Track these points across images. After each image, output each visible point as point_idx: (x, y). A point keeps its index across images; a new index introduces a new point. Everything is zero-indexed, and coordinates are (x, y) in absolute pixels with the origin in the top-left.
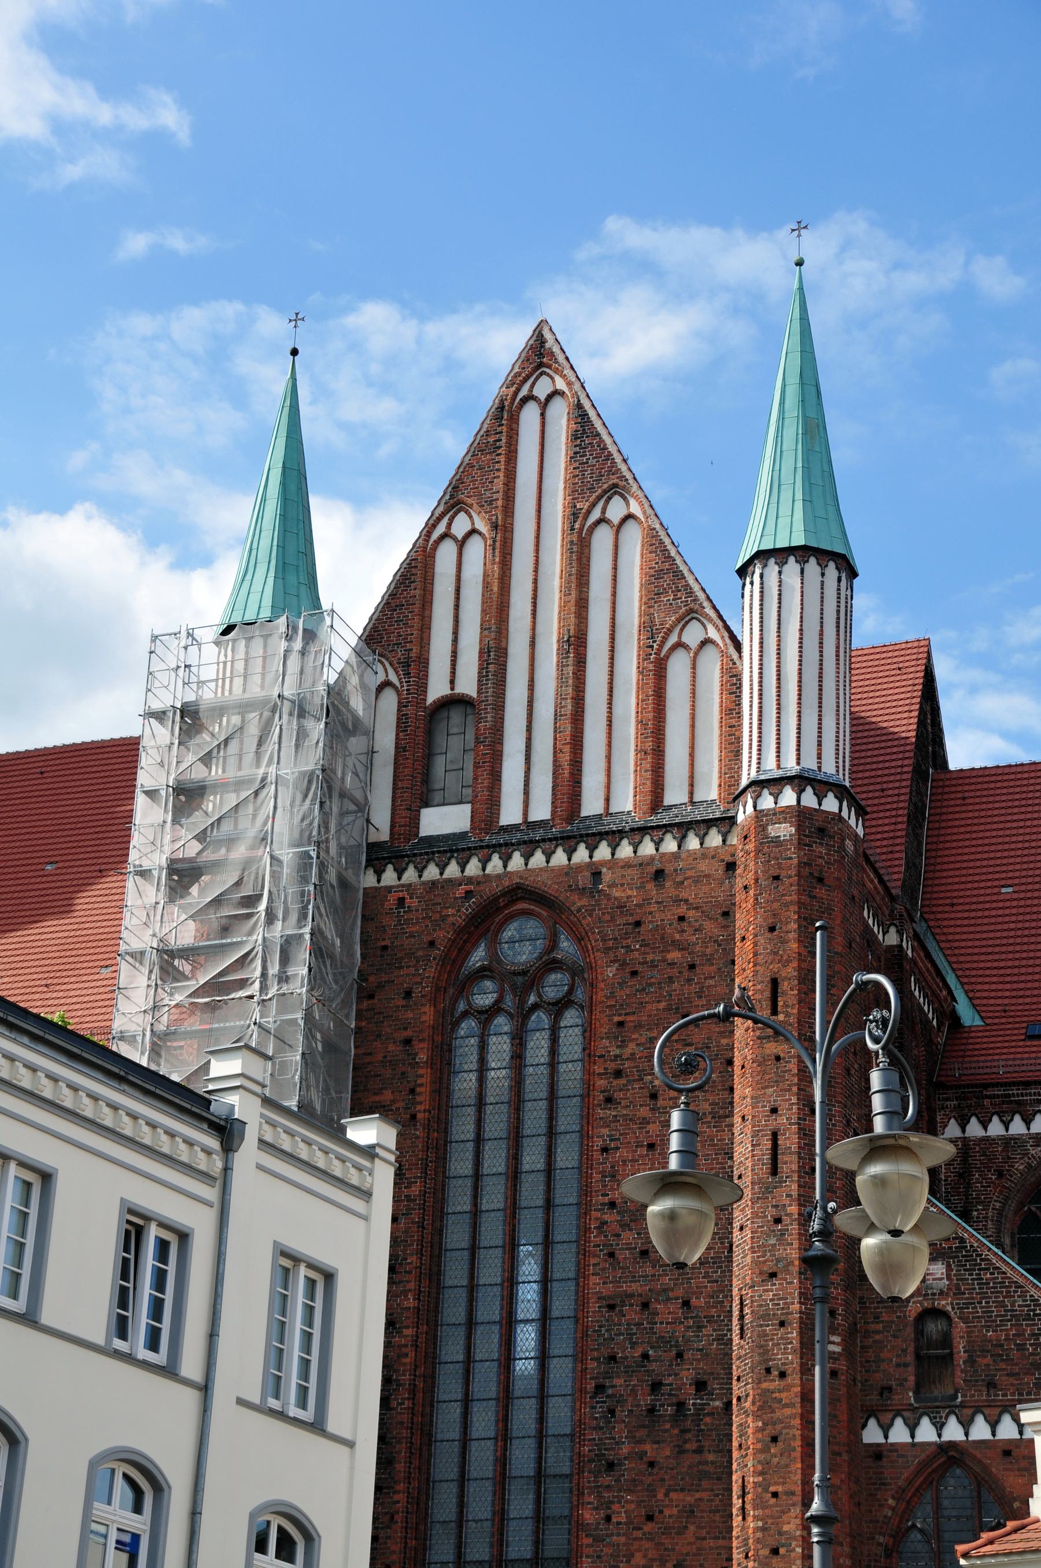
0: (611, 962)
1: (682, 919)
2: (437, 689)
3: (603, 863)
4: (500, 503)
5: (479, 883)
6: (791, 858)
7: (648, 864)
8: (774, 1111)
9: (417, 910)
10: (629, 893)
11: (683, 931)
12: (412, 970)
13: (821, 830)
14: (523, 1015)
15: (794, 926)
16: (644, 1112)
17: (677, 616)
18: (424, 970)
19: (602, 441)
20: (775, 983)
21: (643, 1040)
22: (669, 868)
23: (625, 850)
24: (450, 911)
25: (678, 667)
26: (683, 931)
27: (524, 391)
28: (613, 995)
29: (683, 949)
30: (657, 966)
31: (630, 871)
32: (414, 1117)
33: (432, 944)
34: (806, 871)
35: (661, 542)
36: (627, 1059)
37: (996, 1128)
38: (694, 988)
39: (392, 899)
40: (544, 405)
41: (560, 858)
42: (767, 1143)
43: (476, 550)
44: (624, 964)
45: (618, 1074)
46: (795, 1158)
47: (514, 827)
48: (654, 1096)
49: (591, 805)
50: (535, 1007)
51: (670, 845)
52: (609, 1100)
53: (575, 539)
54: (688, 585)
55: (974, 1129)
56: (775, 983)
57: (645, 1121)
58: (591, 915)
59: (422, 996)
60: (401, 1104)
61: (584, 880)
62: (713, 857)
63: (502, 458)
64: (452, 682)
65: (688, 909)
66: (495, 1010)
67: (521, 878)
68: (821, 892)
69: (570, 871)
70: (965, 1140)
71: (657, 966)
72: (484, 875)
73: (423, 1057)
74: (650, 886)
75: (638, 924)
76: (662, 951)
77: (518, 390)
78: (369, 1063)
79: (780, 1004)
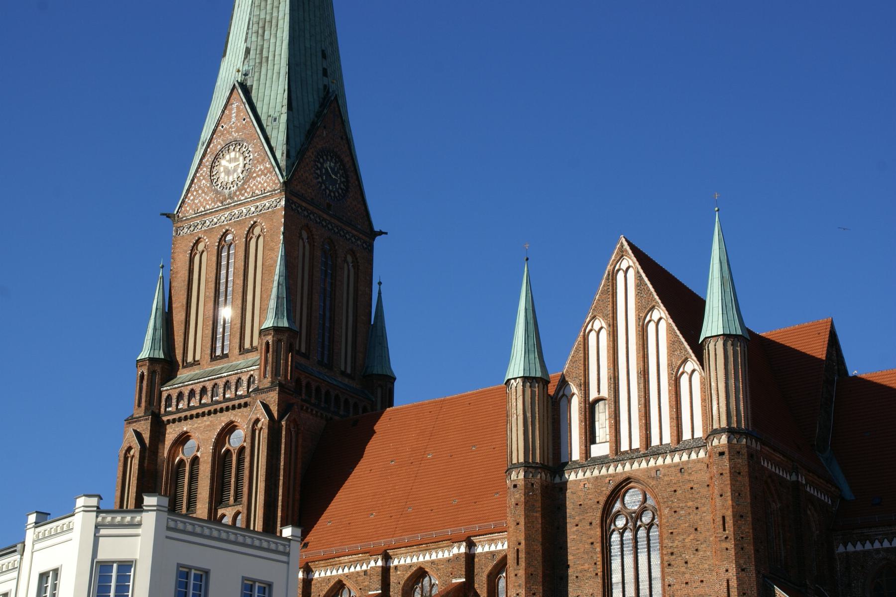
0: (666, 507)
1: (692, 488)
2: (593, 395)
3: (660, 466)
4: (611, 315)
5: (614, 476)
6: (726, 466)
7: (677, 466)
8: (727, 571)
9: (591, 489)
10: (671, 478)
11: (693, 493)
12: (591, 514)
13: (739, 452)
14: (636, 530)
15: (729, 494)
16: (683, 569)
17: (682, 360)
19: (648, 287)
20: (724, 518)
21: (681, 540)
22: (685, 467)
23: (668, 460)
24: (604, 489)
25: (684, 380)
26: (693, 493)
27: (617, 267)
28: (668, 522)
29: (693, 501)
30: (683, 508)
31: (670, 469)
32: (597, 574)
33: (598, 502)
34: (732, 471)
35: (674, 329)
36: (675, 548)
37: (859, 547)
38: (698, 517)
39: (582, 484)
40: (626, 272)
41: (644, 464)
42: (725, 584)
43: (604, 335)
44: (671, 508)
45: (672, 554)
46: (736, 590)
47: (626, 452)
48: (686, 563)
49: (655, 442)
50: (640, 526)
51: (685, 457)
52: (669, 565)
53: (640, 329)
54: (685, 347)
55: (850, 548)
56: (724, 518)
57: (684, 573)
58: (657, 488)
60: (591, 569)
61: (653, 474)
62: (702, 462)
63: (610, 296)
64: (599, 391)
65: (694, 484)
66: (625, 529)
67: (630, 473)
68: (739, 478)
69: (648, 470)
70: (847, 553)
71: (683, 508)
73: (599, 549)
74: (679, 474)
75: (675, 491)
76: (685, 502)
77: (615, 267)
78: (579, 553)
79: (726, 526)
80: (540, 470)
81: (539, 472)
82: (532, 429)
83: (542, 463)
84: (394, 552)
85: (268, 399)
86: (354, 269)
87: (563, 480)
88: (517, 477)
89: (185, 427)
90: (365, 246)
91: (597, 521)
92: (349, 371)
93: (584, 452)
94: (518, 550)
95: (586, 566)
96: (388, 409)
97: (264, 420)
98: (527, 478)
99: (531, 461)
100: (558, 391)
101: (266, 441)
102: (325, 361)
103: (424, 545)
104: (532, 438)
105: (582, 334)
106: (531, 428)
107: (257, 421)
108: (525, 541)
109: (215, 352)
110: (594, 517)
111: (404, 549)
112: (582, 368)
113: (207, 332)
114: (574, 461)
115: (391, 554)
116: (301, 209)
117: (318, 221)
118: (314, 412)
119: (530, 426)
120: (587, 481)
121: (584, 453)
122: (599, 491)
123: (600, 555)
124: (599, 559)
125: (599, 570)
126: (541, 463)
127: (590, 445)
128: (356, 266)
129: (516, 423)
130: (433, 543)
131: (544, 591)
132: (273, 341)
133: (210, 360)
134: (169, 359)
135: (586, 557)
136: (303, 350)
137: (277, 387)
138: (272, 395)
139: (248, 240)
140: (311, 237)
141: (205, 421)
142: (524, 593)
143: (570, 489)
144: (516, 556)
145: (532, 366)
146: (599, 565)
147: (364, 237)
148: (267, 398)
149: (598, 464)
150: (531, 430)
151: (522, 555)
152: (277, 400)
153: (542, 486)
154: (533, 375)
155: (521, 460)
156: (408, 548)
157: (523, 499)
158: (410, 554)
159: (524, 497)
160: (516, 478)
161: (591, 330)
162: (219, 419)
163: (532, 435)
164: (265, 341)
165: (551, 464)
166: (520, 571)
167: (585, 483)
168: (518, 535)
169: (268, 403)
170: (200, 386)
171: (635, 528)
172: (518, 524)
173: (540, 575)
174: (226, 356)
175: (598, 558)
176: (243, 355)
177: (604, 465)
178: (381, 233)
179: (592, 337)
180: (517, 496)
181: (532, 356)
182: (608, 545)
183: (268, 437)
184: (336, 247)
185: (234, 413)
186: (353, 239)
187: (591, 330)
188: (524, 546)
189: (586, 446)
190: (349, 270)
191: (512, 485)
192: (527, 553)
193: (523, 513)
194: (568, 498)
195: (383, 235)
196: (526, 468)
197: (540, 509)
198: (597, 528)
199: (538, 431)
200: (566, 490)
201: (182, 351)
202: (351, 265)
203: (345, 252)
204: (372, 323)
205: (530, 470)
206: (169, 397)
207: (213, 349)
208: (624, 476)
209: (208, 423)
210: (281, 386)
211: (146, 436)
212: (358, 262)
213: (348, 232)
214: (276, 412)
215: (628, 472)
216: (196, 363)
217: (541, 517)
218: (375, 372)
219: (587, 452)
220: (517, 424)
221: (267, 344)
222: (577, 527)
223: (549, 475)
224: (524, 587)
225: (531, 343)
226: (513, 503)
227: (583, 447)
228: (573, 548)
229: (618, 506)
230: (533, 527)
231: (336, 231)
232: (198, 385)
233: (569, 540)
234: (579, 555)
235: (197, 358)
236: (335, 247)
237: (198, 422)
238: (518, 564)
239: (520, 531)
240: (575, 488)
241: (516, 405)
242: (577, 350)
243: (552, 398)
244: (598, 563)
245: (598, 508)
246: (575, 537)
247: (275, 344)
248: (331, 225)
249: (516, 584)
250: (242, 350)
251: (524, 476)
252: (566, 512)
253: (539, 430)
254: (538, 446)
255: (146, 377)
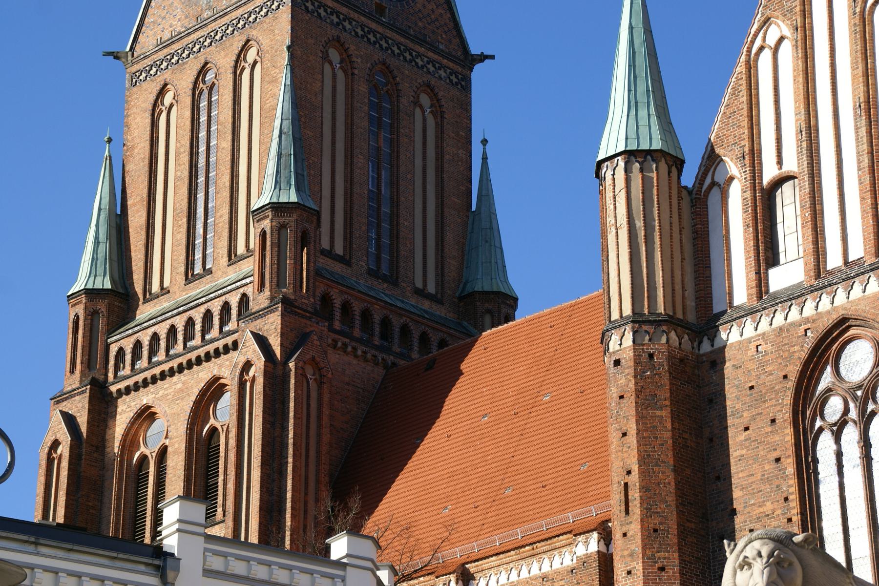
2: (770, 172)
4: (798, 9)
5: (814, 321)
9: (772, 353)
12: (774, 402)
18: (783, 399)
24: (796, 348)
32: (790, 520)
39: (753, 346)
43: (787, 52)
53: (857, 22)
59: (784, 421)
64: (780, 162)
67: (845, 309)
72: (817, 314)
78: (752, 483)
80: (665, 328)
81: (663, 331)
82: (646, 251)
83: (671, 314)
84: (477, 566)
85: (267, 327)
86: (435, 117)
87: (717, 345)
88: (621, 345)
89: (145, 397)
90: (455, 80)
91: (785, 415)
92: (431, 288)
93: (754, 284)
94: (626, 484)
95: (769, 507)
96: (484, 333)
97: (259, 362)
98: (640, 345)
99: (646, 312)
100: (701, 178)
101: (262, 398)
102: (385, 270)
103: (527, 548)
104: (647, 267)
105: (743, 58)
106: (644, 248)
107: (248, 365)
108: (640, 466)
109: (193, 269)
110: (779, 408)
111: (494, 558)
112: (745, 123)
113: (179, 236)
114: (738, 307)
115: (472, 570)
116: (325, 11)
117: (360, 33)
118: (359, 352)
119: (644, 244)
120: (763, 338)
121: (754, 285)
122: (786, 354)
123: (793, 482)
124: (792, 490)
125: (795, 511)
126: (666, 314)
127: (767, 270)
128: (438, 112)
129: (615, 244)
130: (542, 541)
131: (682, 562)
132: (272, 227)
133: (184, 282)
134: (121, 291)
135: (767, 488)
136: (339, 249)
137: (280, 305)
138: (271, 320)
139: (238, 72)
140: (347, 62)
141: (175, 383)
142: (641, 568)
143: (730, 360)
144: (623, 498)
145: (644, 131)
146: (793, 500)
147: (451, 65)
148: (264, 326)
149: (781, 302)
150: (644, 253)
151: (635, 494)
152: (280, 326)
153: (671, 357)
154: (645, 146)
155: (627, 311)
156: (501, 556)
157: (632, 385)
158: (505, 566)
159: (633, 381)
160: (618, 348)
161: (762, 48)
162: (195, 376)
163: (647, 261)
164: (260, 230)
165: (691, 318)
166: (633, 526)
167: (758, 343)
168: (626, 455)
169: (265, 335)
170: (166, 325)
171: (863, 417)
172: (624, 434)
173: (674, 530)
174: (210, 272)
175: (791, 487)
176: (234, 266)
177: (793, 301)
178: (483, 58)
179: (765, 62)
180: (623, 381)
181: (643, 113)
182: (810, 459)
183: (264, 391)
184: (398, 79)
185: (219, 362)
186: (430, 66)
187: (762, 48)
188: (637, 476)
189: (758, 273)
190: (424, 120)
191: (613, 362)
192: (645, 489)
193: (633, 412)
194: (728, 378)
195: (487, 61)
196: (637, 325)
197: (667, 403)
198: (786, 428)
199: (659, 253)
200: (724, 362)
201: (142, 276)
202: (429, 110)
203: (414, 88)
204: (474, 209)
205: (645, 327)
206: (121, 352)
207: (189, 263)
208: (835, 317)
209: (180, 386)
210: (285, 301)
211: (83, 421)
212: (441, 106)
213: (419, 55)
214: (279, 348)
215: (842, 307)
216: (164, 291)
217: (672, 417)
218: (478, 288)
219: (761, 285)
220: (618, 245)
221: (263, 234)
222: (747, 432)
223: (686, 336)
224: (641, 556)
225: (641, 88)
226: (614, 395)
227: (753, 276)
228: (741, 475)
229: (827, 379)
230: (656, 438)
231: (397, 51)
232: (163, 324)
233: (732, 461)
234: (754, 486)
235: (166, 284)
236: (394, 78)
237: (165, 387)
238: (627, 512)
239: (629, 447)
240: (741, 356)
241: (615, 208)
242: (735, 93)
243: (690, 192)
244: (791, 497)
245: (786, 389)
246: (744, 452)
247: (275, 233)
248: (387, 42)
249: (626, 553)
250: (233, 258)
251: (634, 341)
252: (725, 406)
253: (661, 251)
254: (661, 282)
255: (81, 323)
